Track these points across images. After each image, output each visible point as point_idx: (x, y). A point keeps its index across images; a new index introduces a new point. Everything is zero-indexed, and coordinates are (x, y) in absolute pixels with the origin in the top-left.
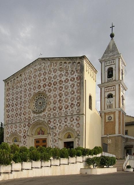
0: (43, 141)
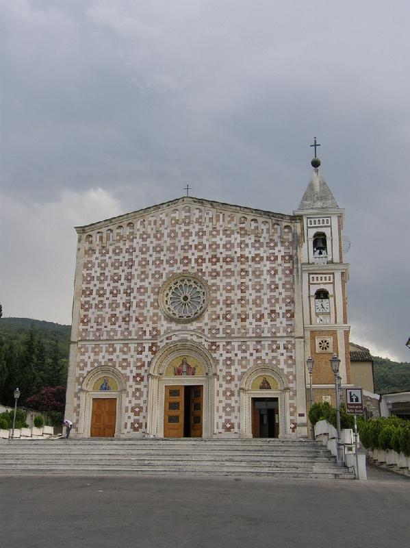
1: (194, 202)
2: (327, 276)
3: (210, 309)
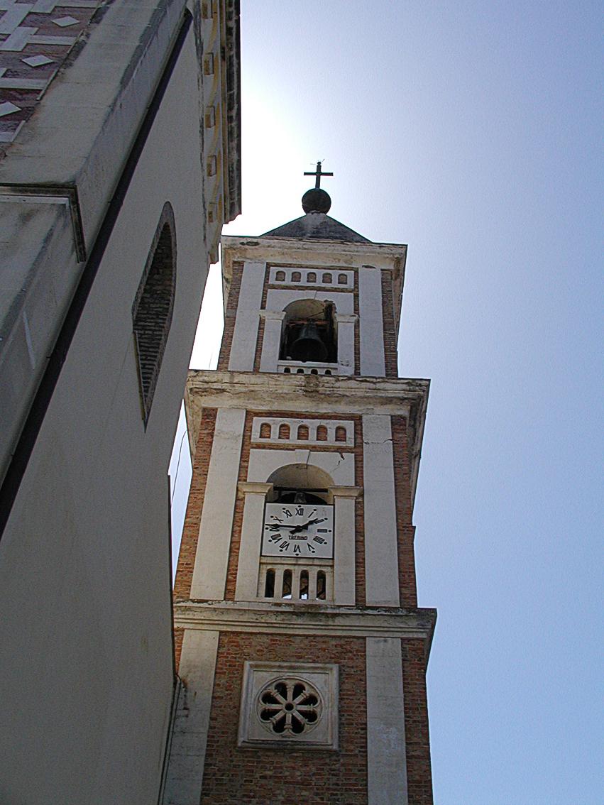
2: (331, 425)
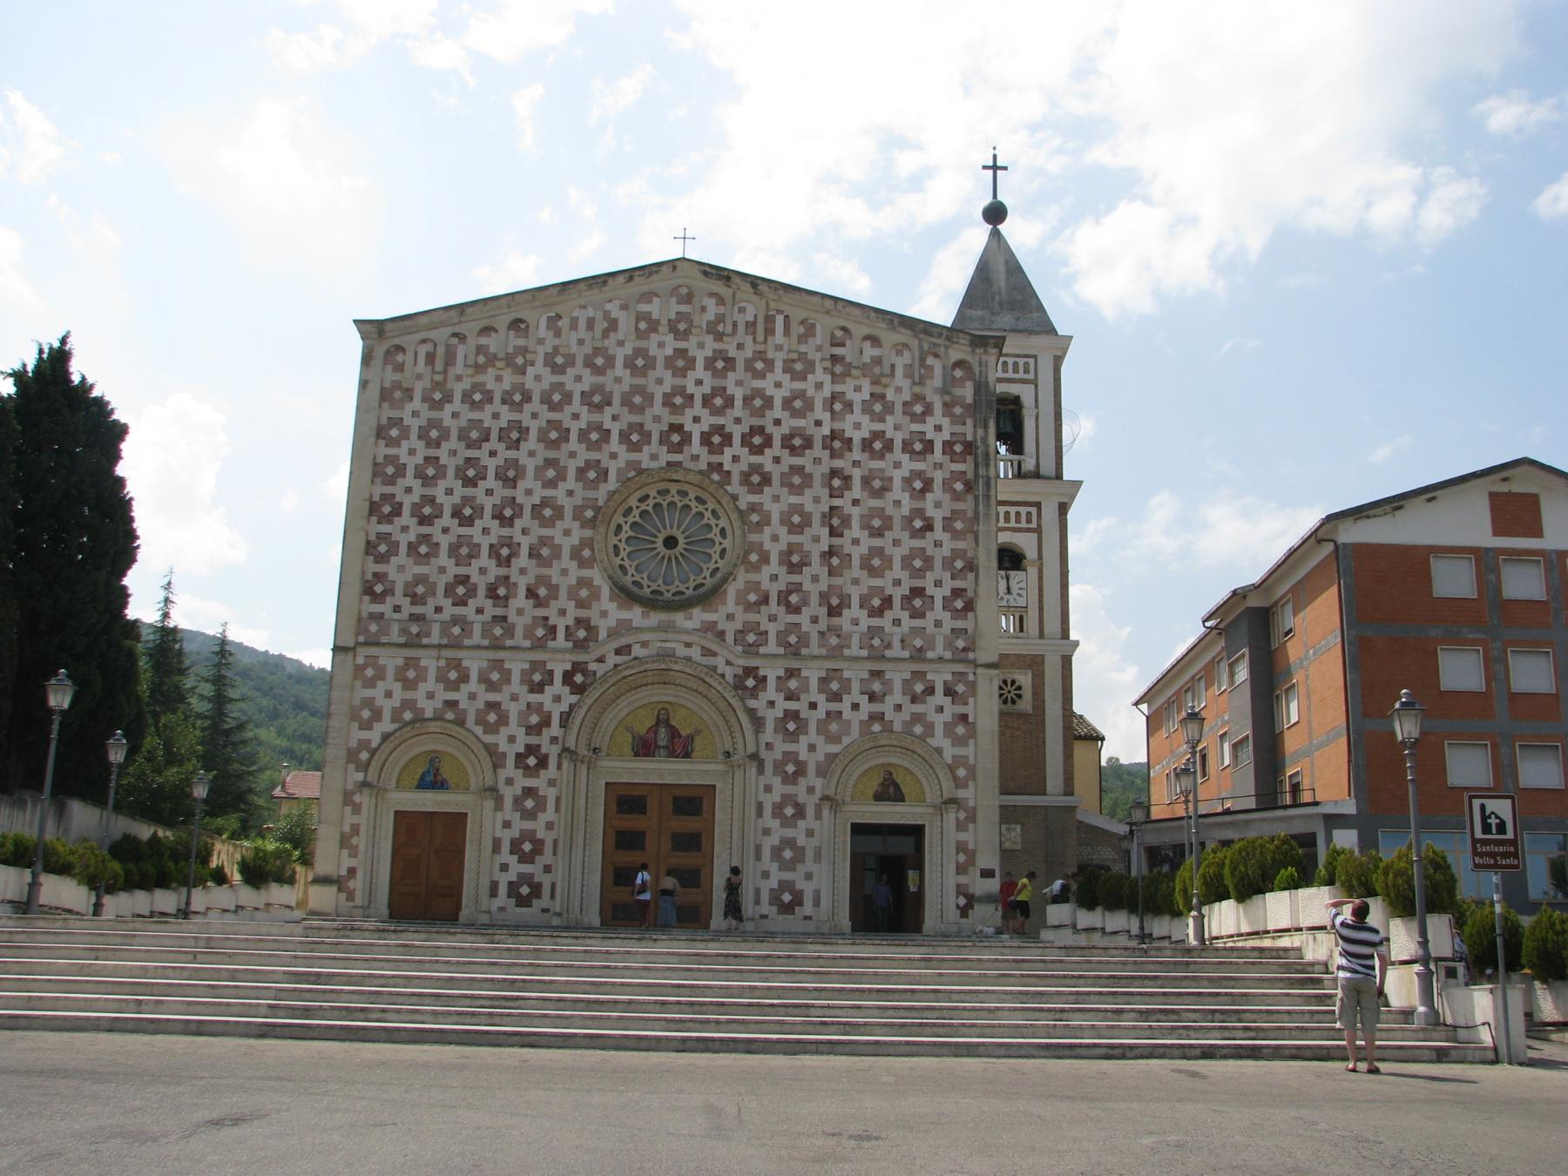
0: (676, 800)
1: (705, 273)
2: (1023, 510)
3: (742, 577)
